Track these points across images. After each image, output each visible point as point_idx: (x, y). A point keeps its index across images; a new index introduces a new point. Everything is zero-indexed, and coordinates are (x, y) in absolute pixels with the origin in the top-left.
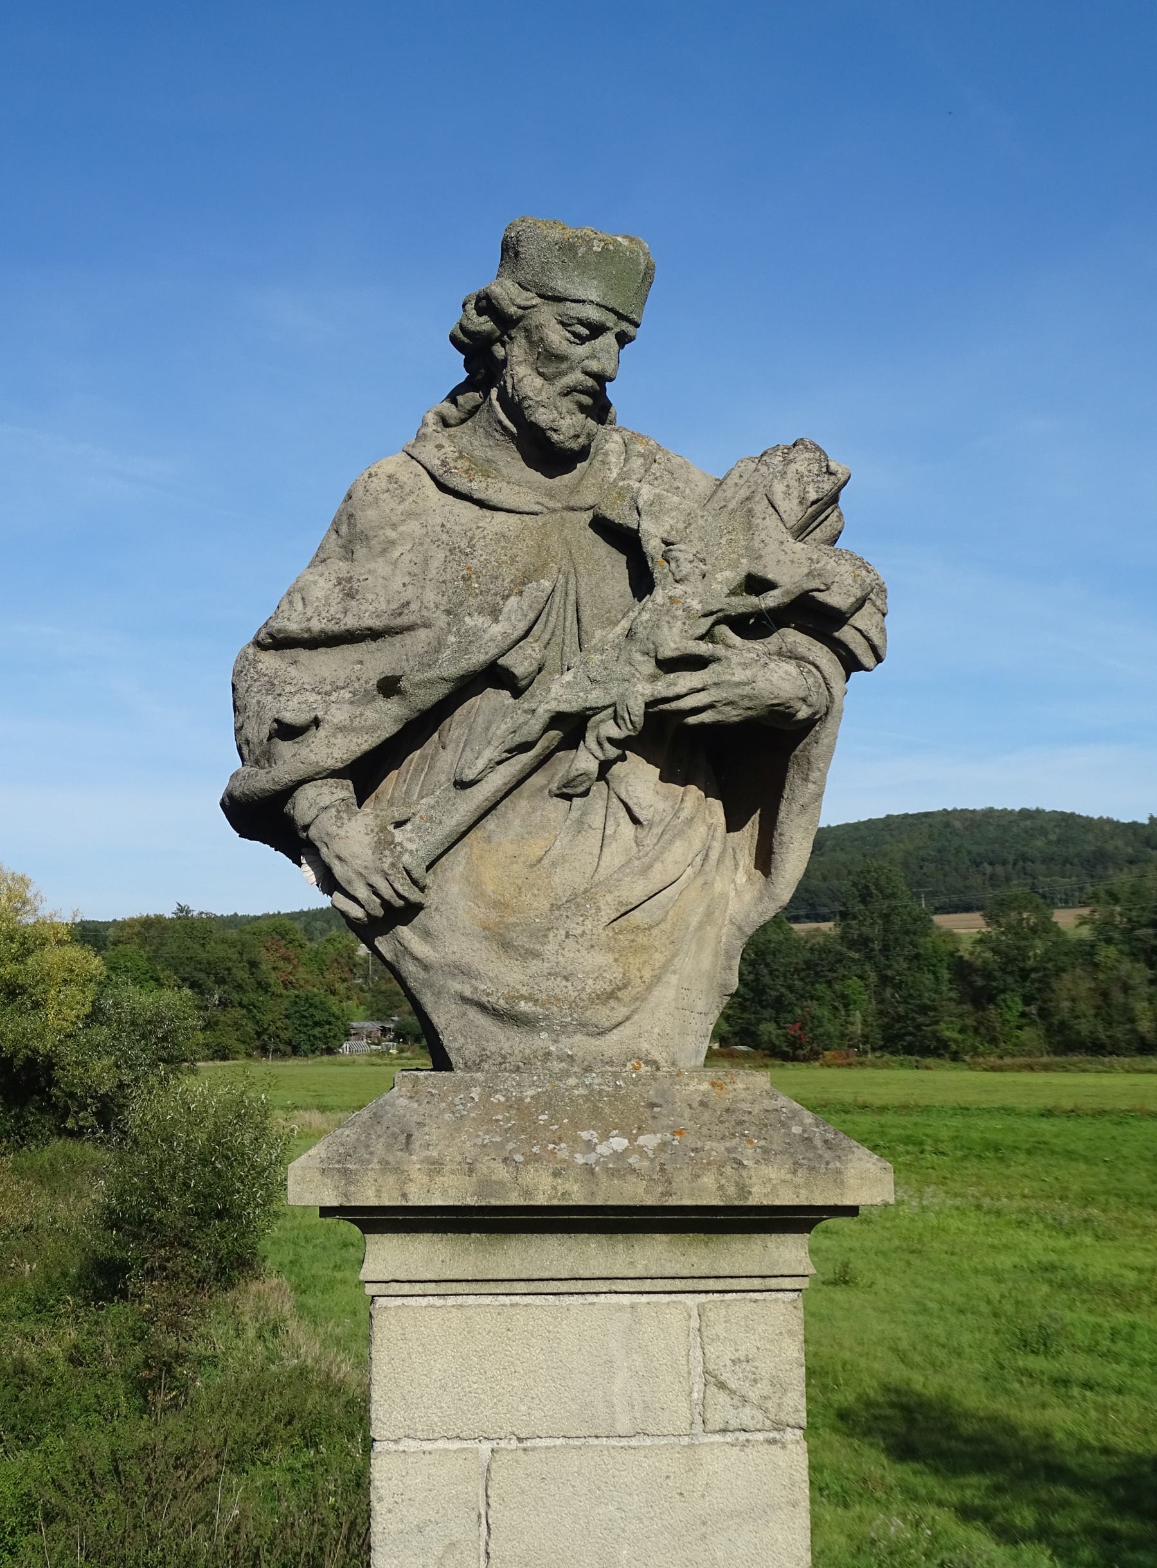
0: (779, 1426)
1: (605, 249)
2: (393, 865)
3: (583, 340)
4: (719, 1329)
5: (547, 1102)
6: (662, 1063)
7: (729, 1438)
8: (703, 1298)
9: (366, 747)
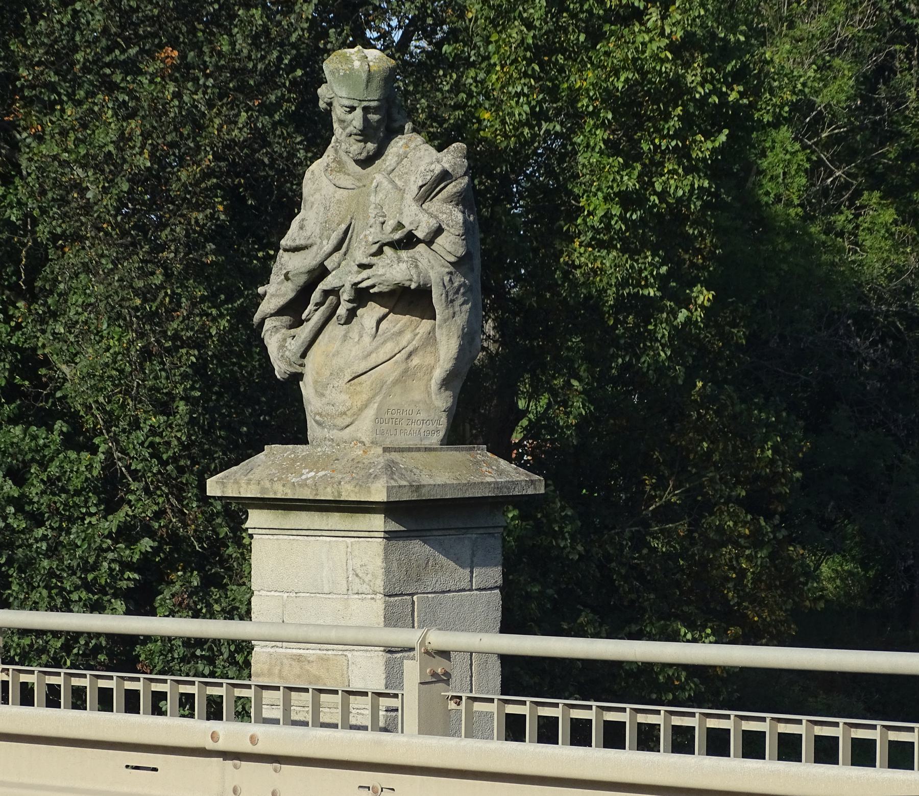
0: (375, 593)
3: (350, 112)
4: (356, 553)
5: (304, 458)
6: (366, 442)
7: (360, 597)
8: (353, 539)
9: (282, 303)
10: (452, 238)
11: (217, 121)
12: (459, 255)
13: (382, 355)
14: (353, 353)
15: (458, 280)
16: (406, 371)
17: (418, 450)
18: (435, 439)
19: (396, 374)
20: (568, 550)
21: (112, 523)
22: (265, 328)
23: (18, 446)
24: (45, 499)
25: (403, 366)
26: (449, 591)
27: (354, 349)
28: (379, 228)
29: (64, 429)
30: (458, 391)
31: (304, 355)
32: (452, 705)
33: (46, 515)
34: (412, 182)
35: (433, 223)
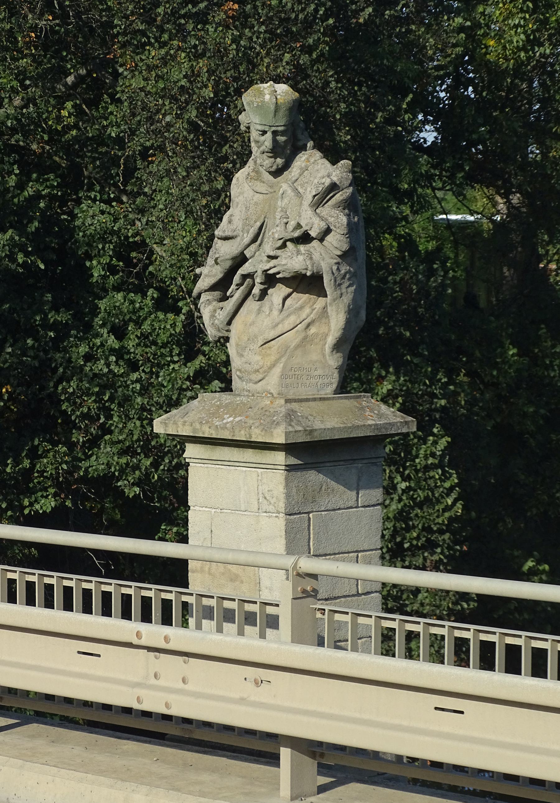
1: (258, 105)
2: (213, 324)
3: (263, 135)
4: (265, 481)
5: (227, 405)
7: (268, 514)
9: (213, 282)
10: (338, 236)
11: (266, 60)
12: (344, 250)
13: (287, 325)
14: (265, 323)
15: (344, 268)
16: (305, 338)
17: (314, 400)
18: (329, 390)
19: (298, 340)
20: (556, 379)
21: (191, 369)
22: (202, 300)
23: (119, 309)
24: (139, 350)
25: (303, 335)
26: (339, 509)
27: (265, 320)
28: (283, 227)
29: (155, 296)
30: (347, 352)
31: (229, 323)
32: (319, 615)
33: (141, 362)
34: (308, 192)
35: (323, 225)
